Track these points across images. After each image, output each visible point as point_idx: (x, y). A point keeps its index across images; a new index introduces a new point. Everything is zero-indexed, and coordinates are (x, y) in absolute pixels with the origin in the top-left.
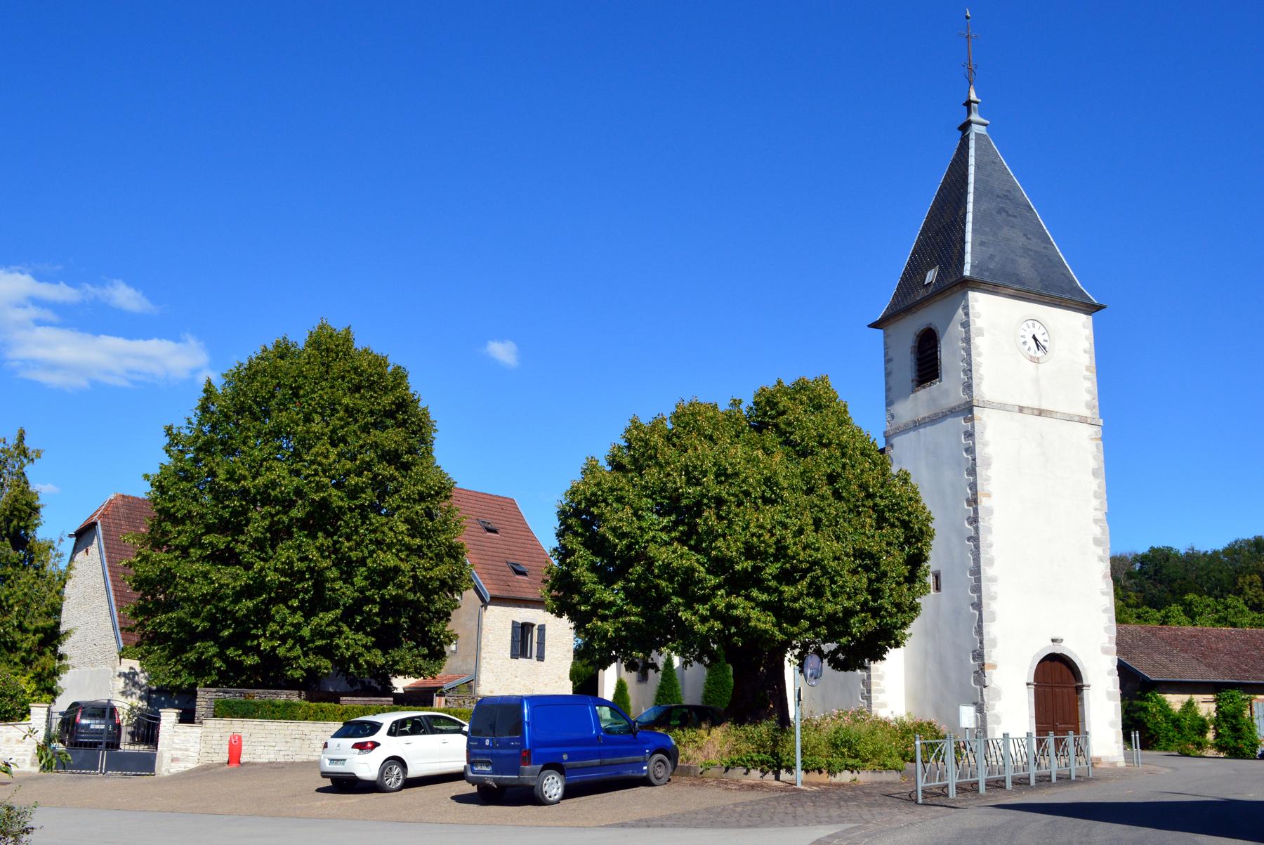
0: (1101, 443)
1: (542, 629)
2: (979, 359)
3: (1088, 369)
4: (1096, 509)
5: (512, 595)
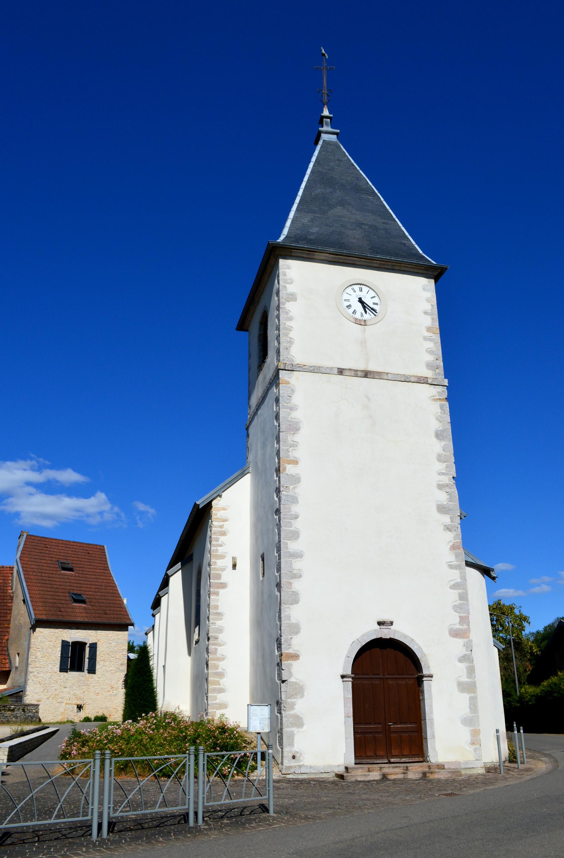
0: (447, 404)
1: (93, 647)
2: (288, 323)
3: (429, 329)
4: (441, 474)
5: (61, 619)
